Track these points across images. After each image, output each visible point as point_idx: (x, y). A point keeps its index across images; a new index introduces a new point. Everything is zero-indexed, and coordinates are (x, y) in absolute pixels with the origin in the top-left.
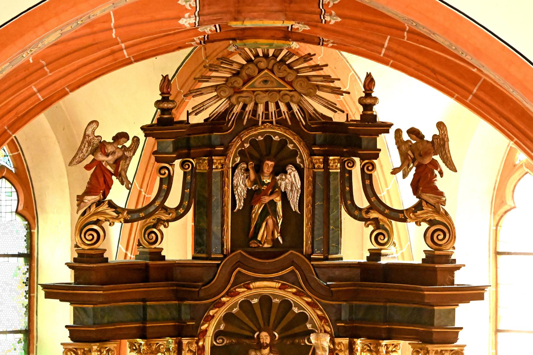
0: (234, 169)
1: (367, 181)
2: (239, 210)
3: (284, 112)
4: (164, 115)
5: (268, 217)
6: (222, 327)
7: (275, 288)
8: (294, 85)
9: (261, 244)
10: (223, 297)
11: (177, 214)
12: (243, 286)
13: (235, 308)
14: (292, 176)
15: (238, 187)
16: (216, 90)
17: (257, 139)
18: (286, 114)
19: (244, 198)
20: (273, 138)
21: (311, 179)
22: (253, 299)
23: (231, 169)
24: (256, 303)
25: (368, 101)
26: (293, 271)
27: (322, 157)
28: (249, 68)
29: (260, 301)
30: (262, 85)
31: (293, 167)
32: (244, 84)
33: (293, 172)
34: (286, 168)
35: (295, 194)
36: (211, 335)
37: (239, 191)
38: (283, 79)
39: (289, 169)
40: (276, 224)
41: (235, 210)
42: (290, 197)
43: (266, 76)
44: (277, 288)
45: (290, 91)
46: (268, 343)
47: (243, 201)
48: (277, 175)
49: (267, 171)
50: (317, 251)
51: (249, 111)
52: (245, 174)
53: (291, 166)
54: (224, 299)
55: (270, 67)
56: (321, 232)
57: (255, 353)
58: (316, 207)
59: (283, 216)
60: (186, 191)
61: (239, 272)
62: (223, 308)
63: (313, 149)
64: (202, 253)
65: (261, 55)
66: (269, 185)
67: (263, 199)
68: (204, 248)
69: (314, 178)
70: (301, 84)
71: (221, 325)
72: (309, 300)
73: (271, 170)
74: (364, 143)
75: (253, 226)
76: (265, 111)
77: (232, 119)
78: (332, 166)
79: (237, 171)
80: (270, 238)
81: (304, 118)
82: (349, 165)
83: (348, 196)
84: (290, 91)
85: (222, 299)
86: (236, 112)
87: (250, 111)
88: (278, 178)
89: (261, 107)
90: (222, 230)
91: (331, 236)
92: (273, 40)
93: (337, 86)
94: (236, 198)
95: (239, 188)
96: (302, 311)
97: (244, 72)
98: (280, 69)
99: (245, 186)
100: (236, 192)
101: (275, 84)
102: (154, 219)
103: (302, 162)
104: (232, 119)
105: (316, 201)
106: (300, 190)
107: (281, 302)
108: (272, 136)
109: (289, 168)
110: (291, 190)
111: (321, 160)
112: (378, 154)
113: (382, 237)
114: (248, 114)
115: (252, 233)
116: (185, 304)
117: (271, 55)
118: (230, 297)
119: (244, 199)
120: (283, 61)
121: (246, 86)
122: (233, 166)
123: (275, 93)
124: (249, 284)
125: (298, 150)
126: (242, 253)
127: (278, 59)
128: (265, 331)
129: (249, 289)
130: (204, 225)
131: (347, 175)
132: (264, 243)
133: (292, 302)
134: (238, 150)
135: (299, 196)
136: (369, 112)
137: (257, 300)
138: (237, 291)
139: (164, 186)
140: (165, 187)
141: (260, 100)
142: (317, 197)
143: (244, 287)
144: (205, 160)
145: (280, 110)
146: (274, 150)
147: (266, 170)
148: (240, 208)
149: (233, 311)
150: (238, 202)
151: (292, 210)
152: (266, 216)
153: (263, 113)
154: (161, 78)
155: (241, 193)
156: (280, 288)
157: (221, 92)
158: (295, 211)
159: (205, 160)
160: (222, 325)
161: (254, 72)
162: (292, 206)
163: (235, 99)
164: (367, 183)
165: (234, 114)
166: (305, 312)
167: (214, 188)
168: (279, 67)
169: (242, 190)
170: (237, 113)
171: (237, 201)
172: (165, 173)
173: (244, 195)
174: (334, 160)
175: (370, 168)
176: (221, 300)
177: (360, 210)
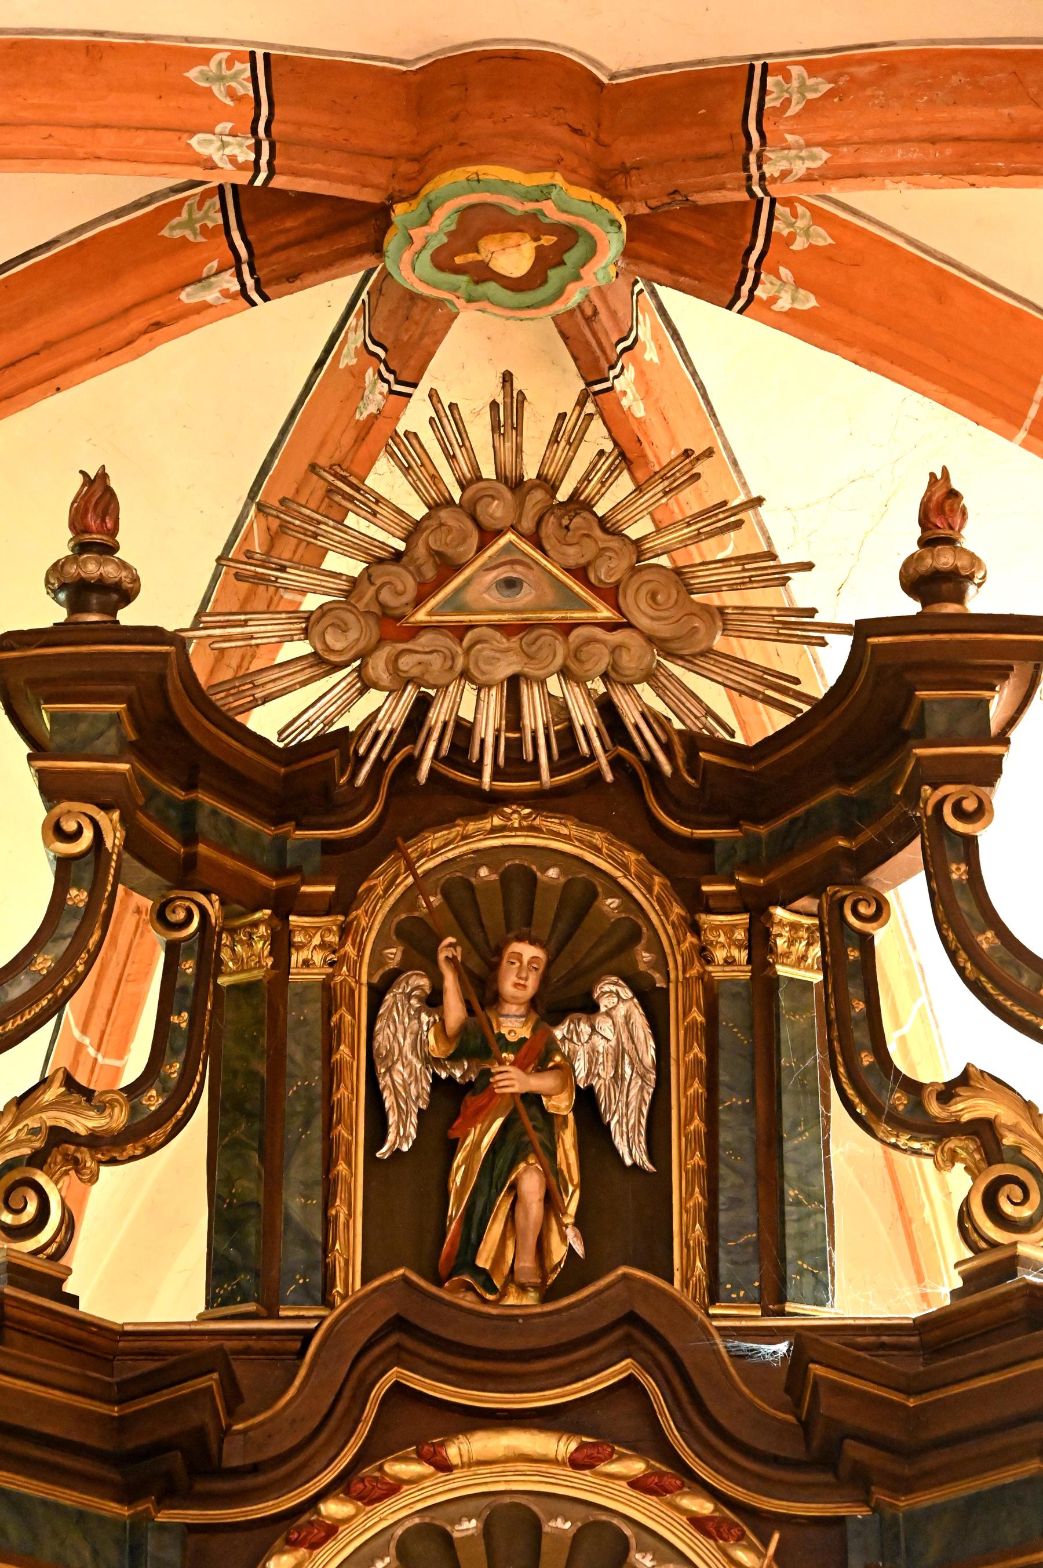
0: (377, 995)
1: (954, 867)
2: (397, 1153)
3: (584, 729)
4: (87, 610)
5: (522, 1166)
7: (554, 1462)
8: (627, 602)
9: (493, 1289)
10: (322, 1496)
11: (134, 1111)
12: (414, 1456)
13: (382, 1559)
14: (620, 1020)
15: (394, 1063)
16: (306, 633)
17: (473, 880)
18: (593, 734)
19: (420, 1110)
20: (538, 874)
21: (697, 1016)
22: (459, 1522)
23: (365, 990)
24: (473, 1535)
25: (945, 559)
26: (630, 1382)
27: (743, 918)
28: (442, 525)
29: (487, 1531)
30: (493, 598)
31: (620, 985)
32: (419, 601)
33: (621, 1005)
34: (590, 994)
35: (634, 1092)
37: (398, 1079)
38: (580, 573)
39: (606, 992)
40: (551, 1202)
41: (383, 1152)
42: (614, 1107)
43: (512, 562)
44: (564, 1464)
45: (611, 627)
47: (414, 1120)
48: (557, 1023)
49: (516, 985)
50: (731, 1291)
51: (439, 726)
52: (424, 1018)
53: (614, 979)
54: (333, 1509)
55: (527, 524)
56: (748, 1214)
58: (723, 1117)
59: (584, 1186)
60: (175, 1019)
61: (398, 1389)
62: (330, 1546)
63: (705, 888)
64: (241, 1302)
65: (488, 471)
66: (525, 1048)
67: (498, 1077)
68: (244, 1278)
69: (711, 1012)
70: (653, 596)
72: (704, 1507)
73: (532, 983)
74: (938, 722)
75: (455, 1210)
76: (507, 730)
77: (373, 755)
78: (787, 955)
79: (389, 997)
80: (527, 1263)
81: (667, 748)
82: (862, 909)
83: (860, 1035)
84: (611, 627)
85: (322, 1507)
86: (389, 727)
87: (445, 724)
88: (559, 1033)
89: (493, 699)
90: (328, 1222)
91: (791, 1228)
92: (549, 174)
93: (801, 603)
94: (387, 1105)
95: (399, 1066)
97: (421, 543)
98: (567, 528)
99: (428, 1060)
100: (388, 1078)
101: (550, 596)
102: (34, 1132)
103: (661, 963)
104: (373, 755)
105: (723, 1092)
106: (653, 1077)
107: (579, 1530)
108: (534, 868)
109: (606, 988)
110: (615, 1077)
111: (740, 935)
112: (1001, 756)
113: (1017, 1193)
114: (436, 735)
115: (452, 1243)
117: (530, 473)
118: (360, 1499)
119: (421, 1113)
120: (579, 504)
121: (432, 603)
122: (375, 980)
123: (548, 631)
124: (442, 1444)
125: (640, 922)
126: (415, 1278)
127: (563, 494)
129: (445, 1467)
130: (248, 1187)
131: (853, 954)
132: (503, 1294)
133: (628, 1531)
134: (397, 920)
135: (648, 1098)
136: (951, 608)
137: (474, 1523)
138: (393, 1477)
139: (74, 892)
140: (78, 896)
141: (484, 667)
142: (723, 1077)
143: (421, 1458)
144: (255, 924)
145: (570, 719)
146: (546, 909)
147: (508, 985)
148: (401, 1144)
150: (392, 1119)
151: (621, 1160)
152: (512, 1165)
153: (497, 739)
154: (77, 483)
155: (406, 1086)
156: (576, 1463)
157: (329, 630)
158: (635, 1164)
159: (255, 924)
161: (464, 539)
162: (623, 1149)
163: (387, 666)
164: (955, 876)
165: (377, 734)
167: (295, 1051)
168: (565, 522)
169: (410, 1075)
170: (392, 732)
171: (391, 1113)
172: (78, 833)
173: (418, 1098)
174: (794, 927)
175: (970, 805)
176: (318, 1512)
177: (914, 1088)
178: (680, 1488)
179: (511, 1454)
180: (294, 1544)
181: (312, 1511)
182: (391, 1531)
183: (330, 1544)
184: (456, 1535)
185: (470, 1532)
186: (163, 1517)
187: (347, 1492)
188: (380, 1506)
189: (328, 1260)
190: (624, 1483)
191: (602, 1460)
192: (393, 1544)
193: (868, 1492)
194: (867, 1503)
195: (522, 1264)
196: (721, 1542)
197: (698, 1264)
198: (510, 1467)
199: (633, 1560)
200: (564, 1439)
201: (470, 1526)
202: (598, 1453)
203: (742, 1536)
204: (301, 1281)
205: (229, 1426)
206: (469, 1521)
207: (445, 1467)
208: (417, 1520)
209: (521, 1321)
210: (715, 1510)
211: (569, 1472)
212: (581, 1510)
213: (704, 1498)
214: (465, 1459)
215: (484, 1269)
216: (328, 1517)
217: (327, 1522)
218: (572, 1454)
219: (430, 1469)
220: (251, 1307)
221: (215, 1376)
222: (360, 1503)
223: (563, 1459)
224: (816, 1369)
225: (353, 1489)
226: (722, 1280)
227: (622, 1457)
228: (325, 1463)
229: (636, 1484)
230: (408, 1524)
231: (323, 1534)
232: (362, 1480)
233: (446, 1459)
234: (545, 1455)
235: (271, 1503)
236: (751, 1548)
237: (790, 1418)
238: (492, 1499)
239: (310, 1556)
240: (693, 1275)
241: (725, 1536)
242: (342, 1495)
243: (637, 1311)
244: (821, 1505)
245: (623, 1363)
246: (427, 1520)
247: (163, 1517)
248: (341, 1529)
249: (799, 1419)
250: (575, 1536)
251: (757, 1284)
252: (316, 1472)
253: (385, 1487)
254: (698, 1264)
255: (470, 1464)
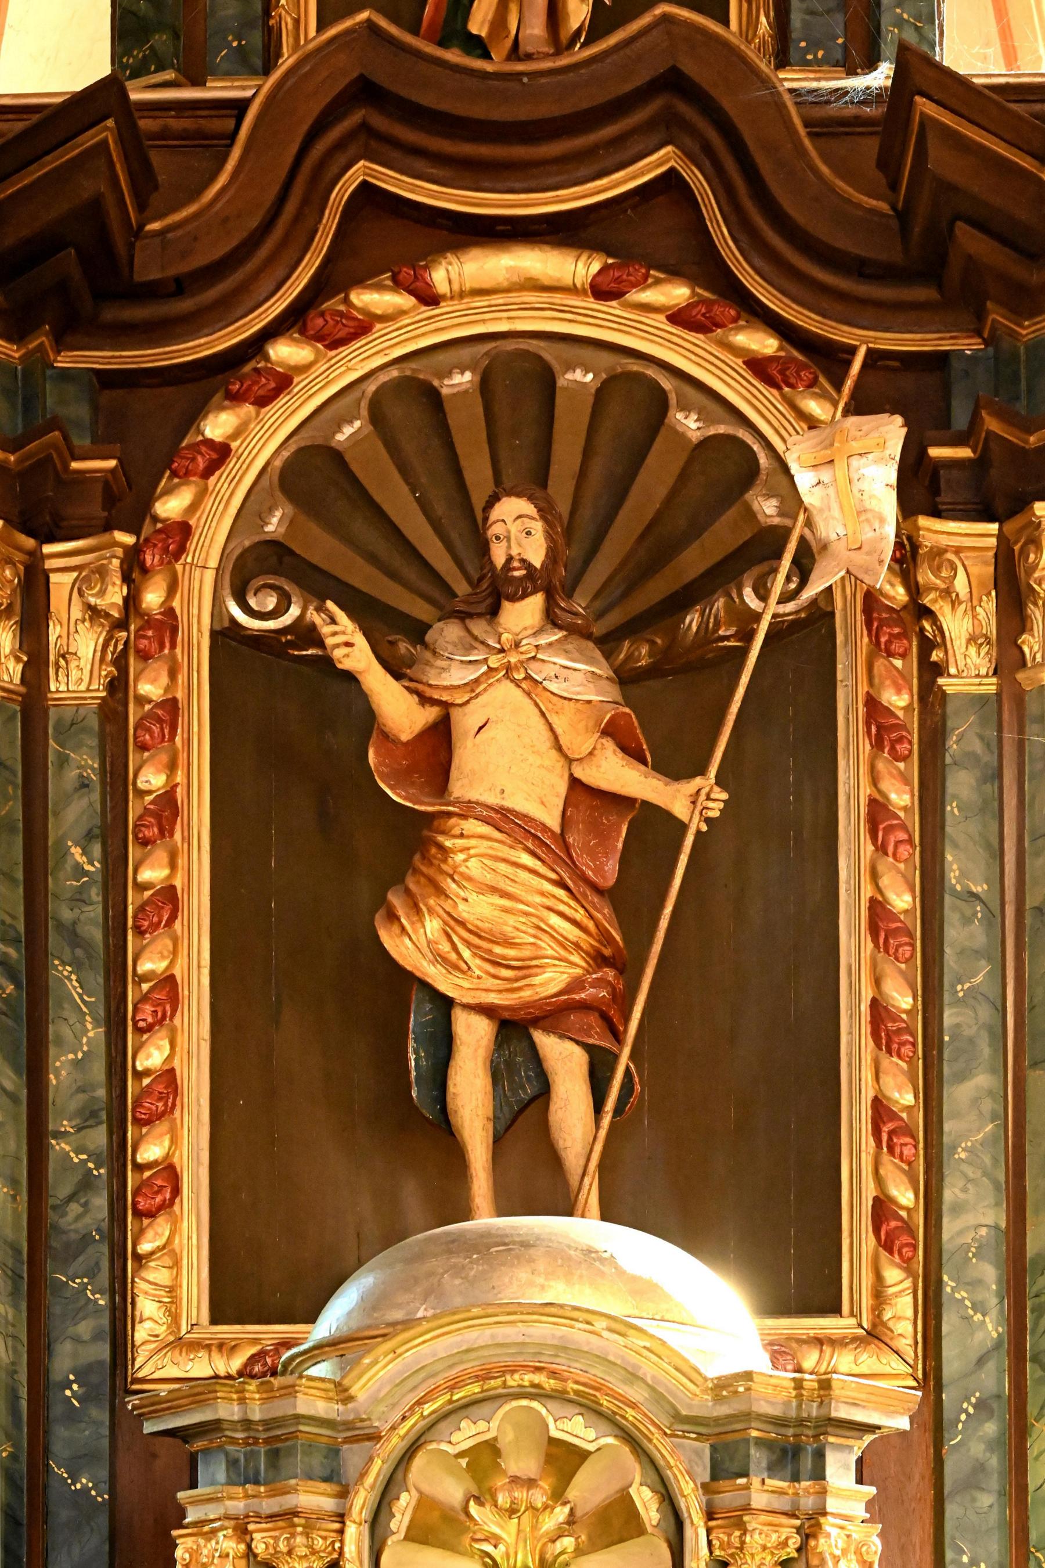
6: (274, 525)
7: (572, 290)
12: (389, 283)
13: (350, 422)
22: (449, 374)
24: (466, 392)
29: (485, 385)
36: (213, 563)
44: (584, 292)
46: (537, 559)
57: (462, 633)
71: (271, 511)
96: (722, 429)
107: (605, 383)
116: (65, 375)
118: (319, 338)
124: (426, 267)
128: (519, 495)
129: (429, 298)
133: (667, 383)
137: (468, 376)
143: (398, 285)
149: (340, 437)
160: (278, 514)
166: (743, 434)
176: (267, 359)
178: (735, 320)
179: (515, 279)
180: (236, 398)
181: (258, 358)
182: (363, 386)
183: (282, 400)
184: (445, 391)
185: (463, 387)
186: (64, 361)
187: (303, 332)
188: (345, 351)
189: (272, 22)
190: (662, 317)
191: (634, 286)
192: (364, 404)
193: (980, 315)
194: (978, 333)
195: (528, 32)
196: (786, 389)
197: (763, 19)
198: (515, 297)
199: (673, 420)
200: (584, 257)
201: (463, 379)
202: (629, 275)
203: (813, 383)
204: (235, 44)
205: (141, 226)
206: (462, 373)
207: (429, 298)
208: (394, 373)
209: (525, 80)
210: (780, 348)
211: (591, 303)
212: (607, 359)
213: (765, 332)
214: (456, 287)
215: (478, 38)
216: (280, 364)
217: (279, 369)
218: (595, 277)
219: (412, 301)
220: (169, 75)
221: (110, 123)
222: (319, 345)
223: (583, 284)
224: (923, 105)
225: (309, 324)
226: (794, 35)
227: (658, 282)
228: (272, 287)
229: (678, 317)
230: (383, 378)
231: (273, 385)
232: (322, 314)
233: (430, 286)
234: (559, 280)
235: (202, 341)
236: (824, 396)
237: (884, 206)
238: (490, 346)
239: (258, 414)
240: (755, 35)
241: (792, 380)
242: (296, 335)
243: (683, 68)
244: (919, 336)
245: (662, 152)
246: (408, 373)
247: (64, 361)
248: (296, 380)
249: (894, 208)
250: (599, 391)
251: (840, 41)
252: (261, 298)
253: (351, 323)
254: (763, 19)
255: (462, 295)
